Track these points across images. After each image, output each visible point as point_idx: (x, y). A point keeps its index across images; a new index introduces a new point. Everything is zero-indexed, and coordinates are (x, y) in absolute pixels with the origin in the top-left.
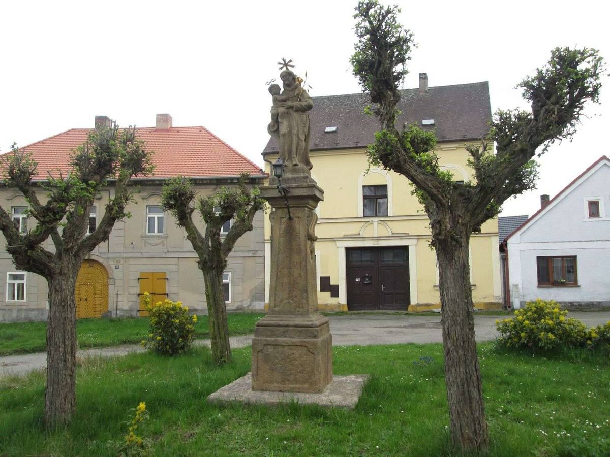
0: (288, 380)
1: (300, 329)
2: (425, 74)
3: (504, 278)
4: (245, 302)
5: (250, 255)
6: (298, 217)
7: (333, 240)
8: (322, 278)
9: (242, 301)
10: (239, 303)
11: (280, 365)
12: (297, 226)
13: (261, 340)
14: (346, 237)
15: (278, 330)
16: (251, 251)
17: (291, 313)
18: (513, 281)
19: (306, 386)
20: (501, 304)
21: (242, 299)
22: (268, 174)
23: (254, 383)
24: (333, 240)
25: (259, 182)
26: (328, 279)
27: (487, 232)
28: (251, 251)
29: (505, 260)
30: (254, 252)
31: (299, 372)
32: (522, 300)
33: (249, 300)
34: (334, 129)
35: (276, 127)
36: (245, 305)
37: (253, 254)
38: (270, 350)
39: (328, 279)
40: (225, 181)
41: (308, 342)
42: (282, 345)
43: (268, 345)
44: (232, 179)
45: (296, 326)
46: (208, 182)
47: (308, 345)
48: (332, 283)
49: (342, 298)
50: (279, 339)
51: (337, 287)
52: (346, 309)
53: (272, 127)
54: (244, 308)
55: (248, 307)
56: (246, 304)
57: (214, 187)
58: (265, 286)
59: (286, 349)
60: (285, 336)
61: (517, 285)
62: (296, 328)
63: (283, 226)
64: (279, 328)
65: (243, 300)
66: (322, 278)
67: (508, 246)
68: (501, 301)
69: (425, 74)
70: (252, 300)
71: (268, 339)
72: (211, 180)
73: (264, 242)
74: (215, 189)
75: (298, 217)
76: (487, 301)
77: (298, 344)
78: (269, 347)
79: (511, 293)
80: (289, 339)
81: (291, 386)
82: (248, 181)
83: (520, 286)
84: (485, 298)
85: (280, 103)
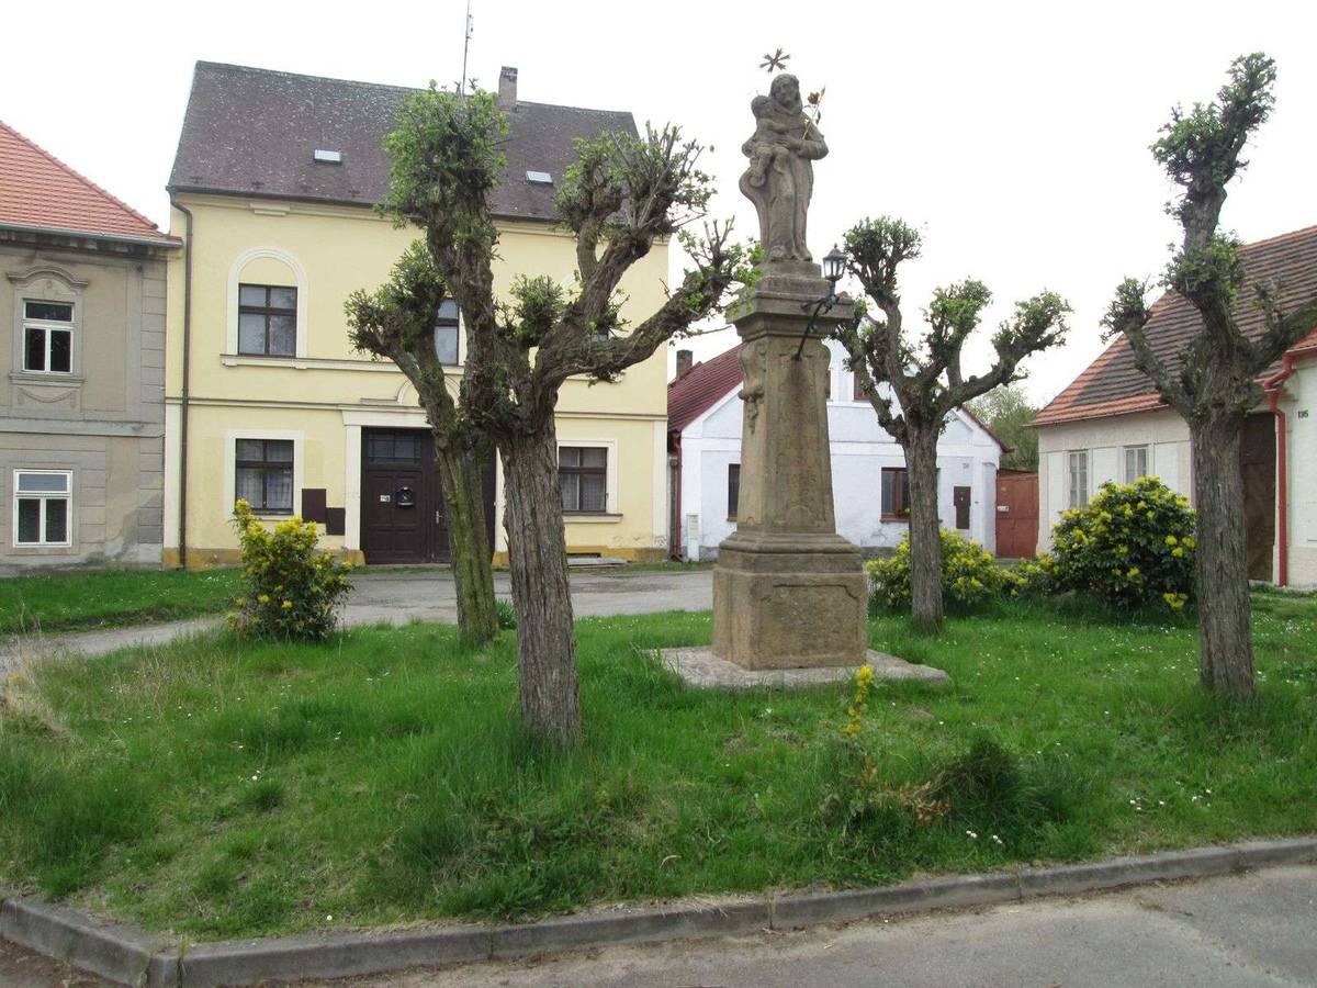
0: (814, 647)
1: (832, 556)
2: (515, 71)
3: (673, 502)
4: (110, 545)
5: (127, 431)
6: (810, 357)
7: (337, 408)
8: (305, 492)
9: (101, 543)
10: (94, 549)
11: (801, 622)
12: (809, 373)
13: (768, 577)
14: (365, 405)
15: (797, 559)
16: (131, 422)
17: (806, 529)
18: (688, 507)
19: (842, 654)
20: (664, 550)
21: (102, 538)
22: (179, 239)
23: (755, 657)
24: (337, 408)
25: (154, 255)
26: (321, 494)
27: (649, 413)
28: (131, 422)
29: (675, 468)
30: (134, 425)
31: (834, 632)
32: (701, 544)
33: (120, 541)
34: (334, 156)
35: (762, 182)
36: (108, 553)
37: (134, 429)
38: (784, 594)
39: (321, 494)
40: (62, 243)
41: (849, 579)
42: (803, 586)
43: (782, 585)
44: (82, 240)
45: (825, 552)
46: (13, 239)
47: (848, 584)
48: (330, 504)
49: (352, 538)
50: (800, 574)
51: (340, 513)
52: (360, 560)
53: (757, 178)
54: (108, 558)
55: (118, 556)
56: (112, 549)
57: (27, 252)
58: (163, 507)
59: (812, 592)
60: (807, 570)
61: (695, 516)
62: (826, 555)
63: (785, 371)
64: (796, 555)
65: (106, 540)
66: (305, 492)
67: (683, 441)
68: (665, 545)
69: (515, 71)
70: (128, 542)
71: (780, 575)
72: (20, 232)
73: (163, 402)
74: (30, 259)
75: (810, 357)
76: (639, 545)
77: (832, 582)
78: (782, 589)
79: (683, 530)
80: (814, 574)
81: (818, 656)
82: (126, 250)
83: (700, 517)
84: (637, 540)
85: (776, 136)
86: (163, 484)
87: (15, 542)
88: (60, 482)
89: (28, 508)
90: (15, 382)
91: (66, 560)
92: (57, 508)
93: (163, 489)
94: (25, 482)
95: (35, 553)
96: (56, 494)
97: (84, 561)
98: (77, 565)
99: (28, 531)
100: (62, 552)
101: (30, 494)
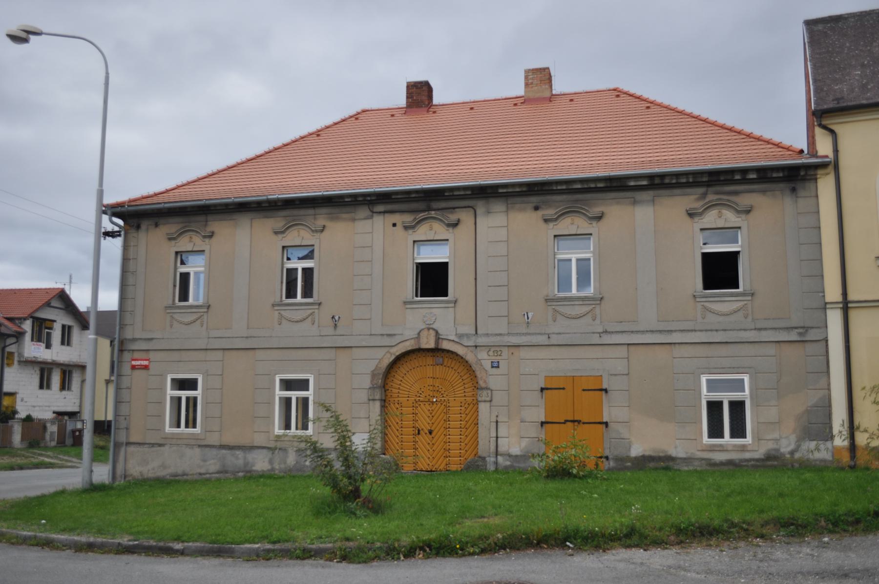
4: (784, 442)
5: (793, 336)
9: (777, 440)
10: (771, 445)
16: (796, 328)
21: (778, 437)
22: (827, 157)
25: (806, 174)
28: (796, 328)
30: (801, 330)
33: (793, 438)
36: (782, 450)
37: (800, 334)
40: (729, 177)
44: (744, 171)
46: (691, 180)
54: (783, 455)
55: (792, 453)
56: (786, 447)
57: (701, 190)
58: (830, 406)
65: (781, 437)
70: (800, 440)
73: (825, 307)
74: (704, 196)
82: (781, 175)
86: (829, 385)
87: (706, 439)
88: (738, 385)
89: (714, 407)
90: (698, 300)
91: (747, 455)
92: (737, 407)
93: (829, 389)
94: (712, 385)
95: (722, 449)
96: (736, 396)
97: (762, 457)
98: (757, 460)
99: (715, 431)
100: (743, 448)
101: (716, 396)
